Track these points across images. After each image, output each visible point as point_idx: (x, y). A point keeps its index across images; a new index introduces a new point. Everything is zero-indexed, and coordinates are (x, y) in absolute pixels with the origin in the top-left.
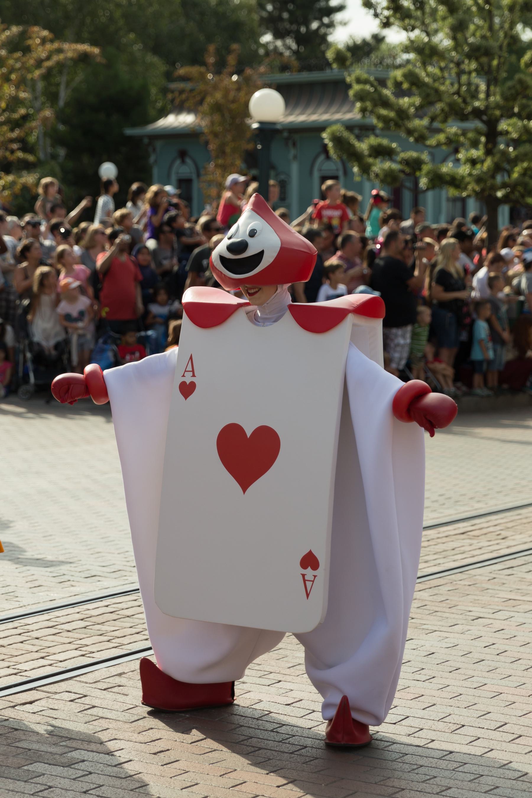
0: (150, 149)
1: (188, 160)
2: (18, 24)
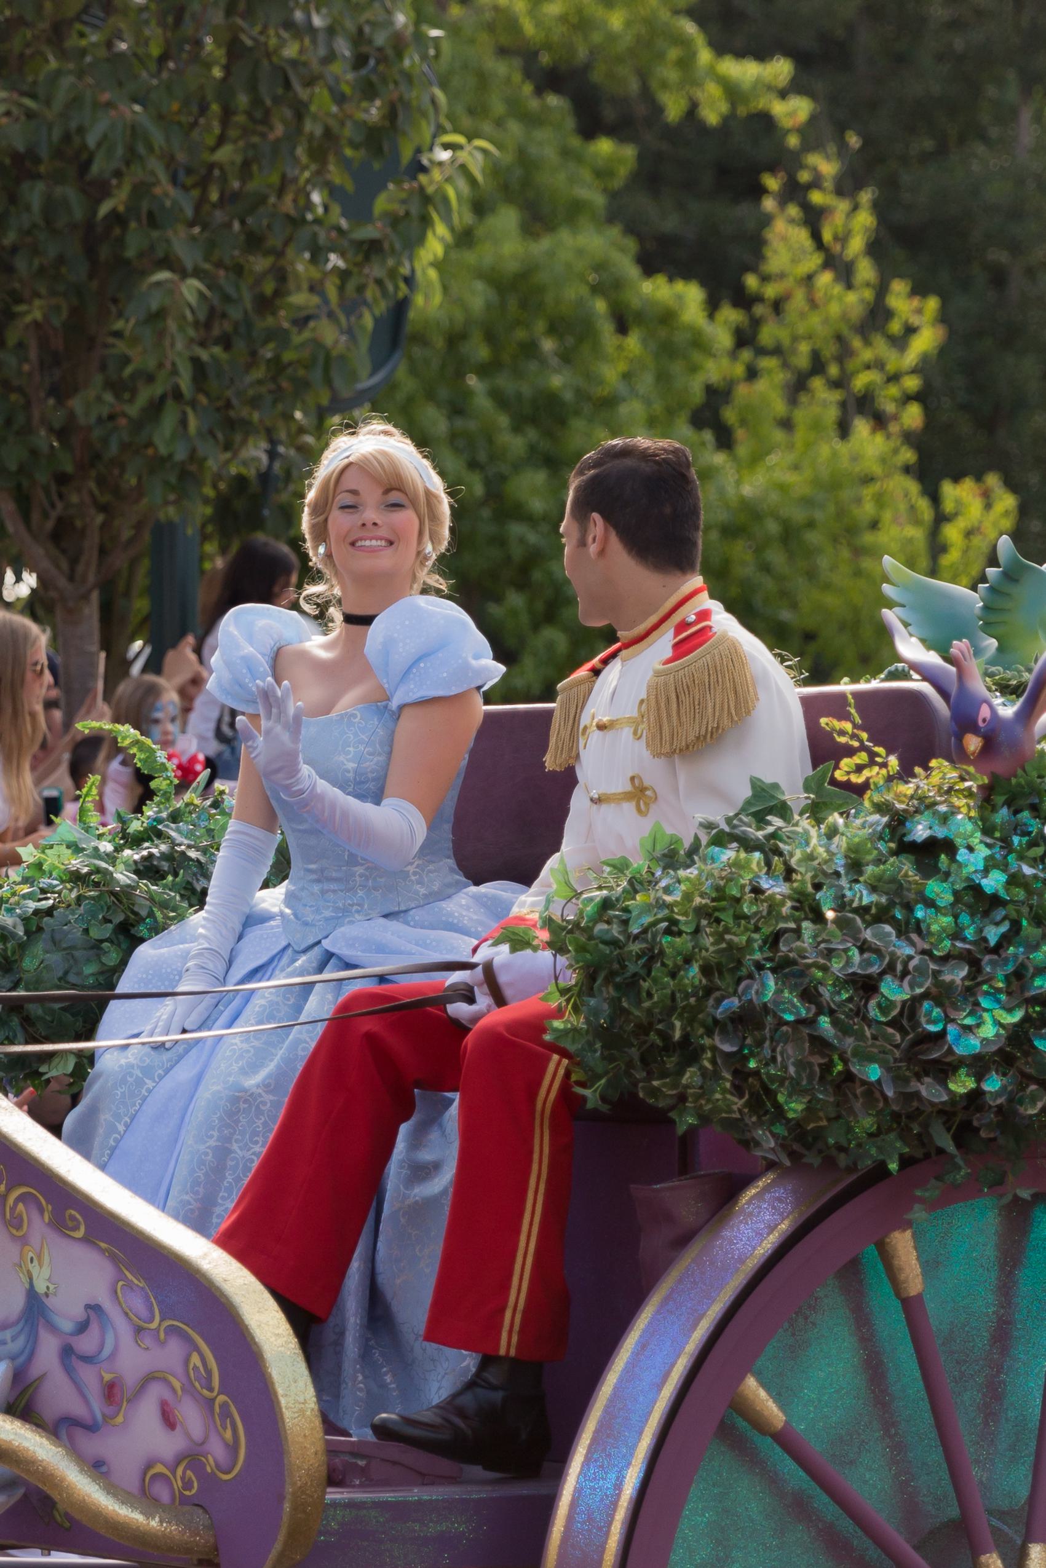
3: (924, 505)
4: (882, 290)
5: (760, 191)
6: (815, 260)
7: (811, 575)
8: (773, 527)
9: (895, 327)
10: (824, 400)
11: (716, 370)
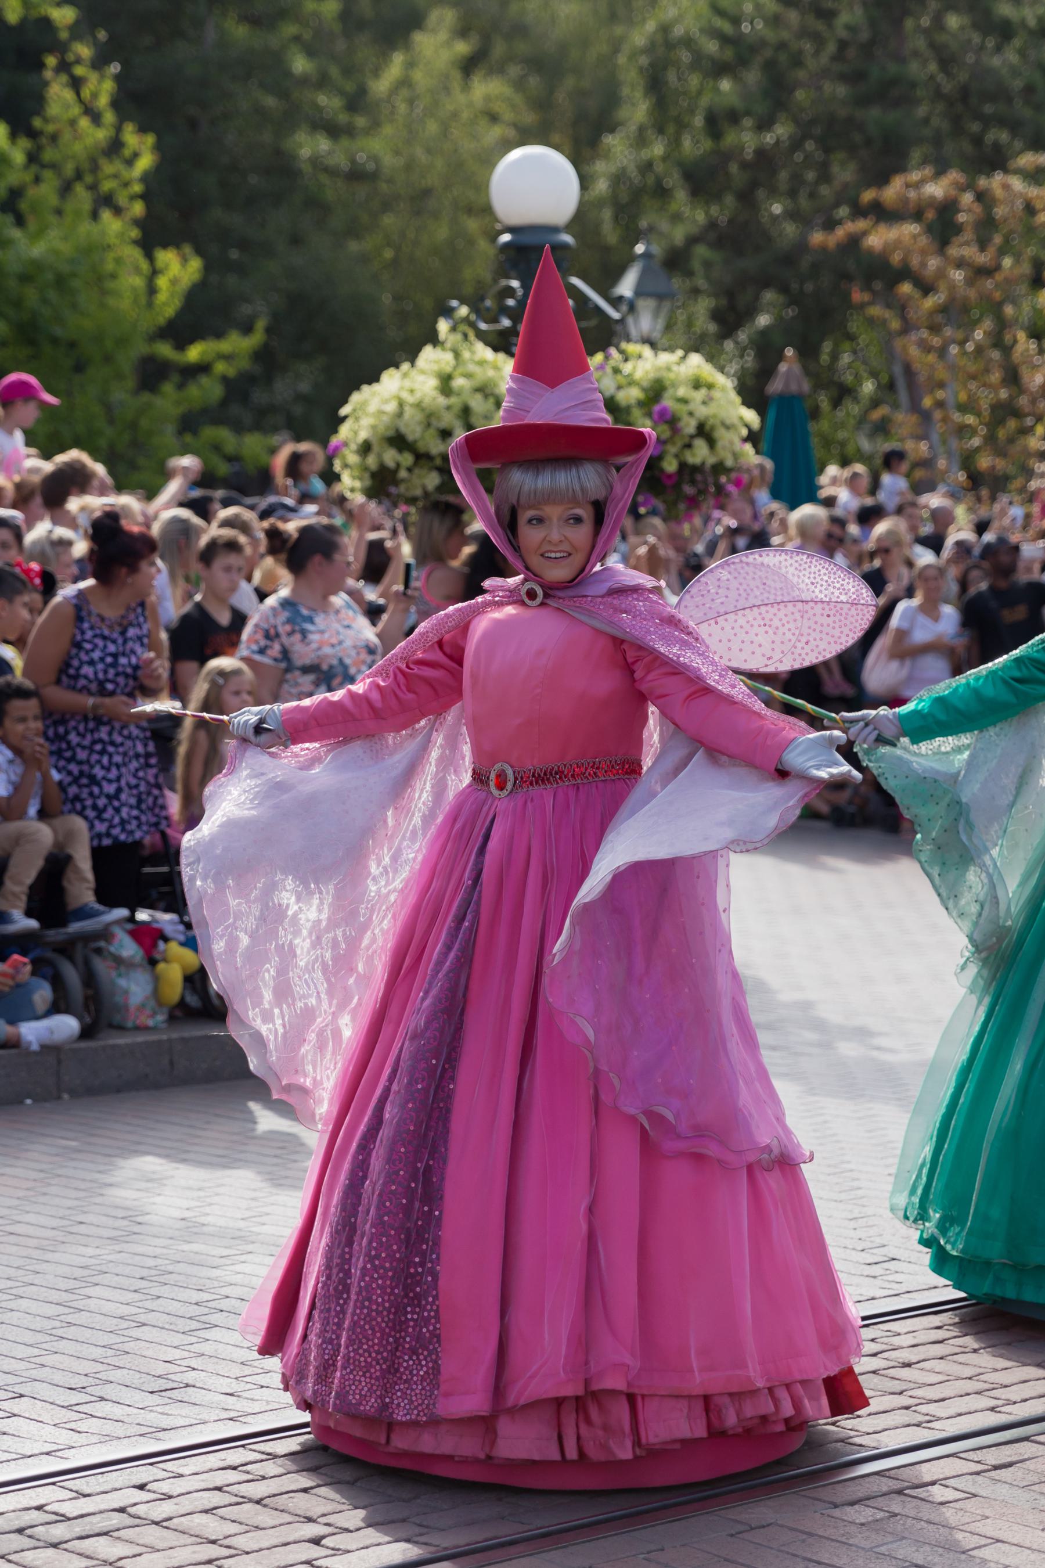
3: (144, 265)
4: (119, 129)
5: (42, 65)
6: (76, 110)
7: (74, 306)
8: (50, 276)
9: (127, 152)
10: (82, 196)
11: (14, 178)
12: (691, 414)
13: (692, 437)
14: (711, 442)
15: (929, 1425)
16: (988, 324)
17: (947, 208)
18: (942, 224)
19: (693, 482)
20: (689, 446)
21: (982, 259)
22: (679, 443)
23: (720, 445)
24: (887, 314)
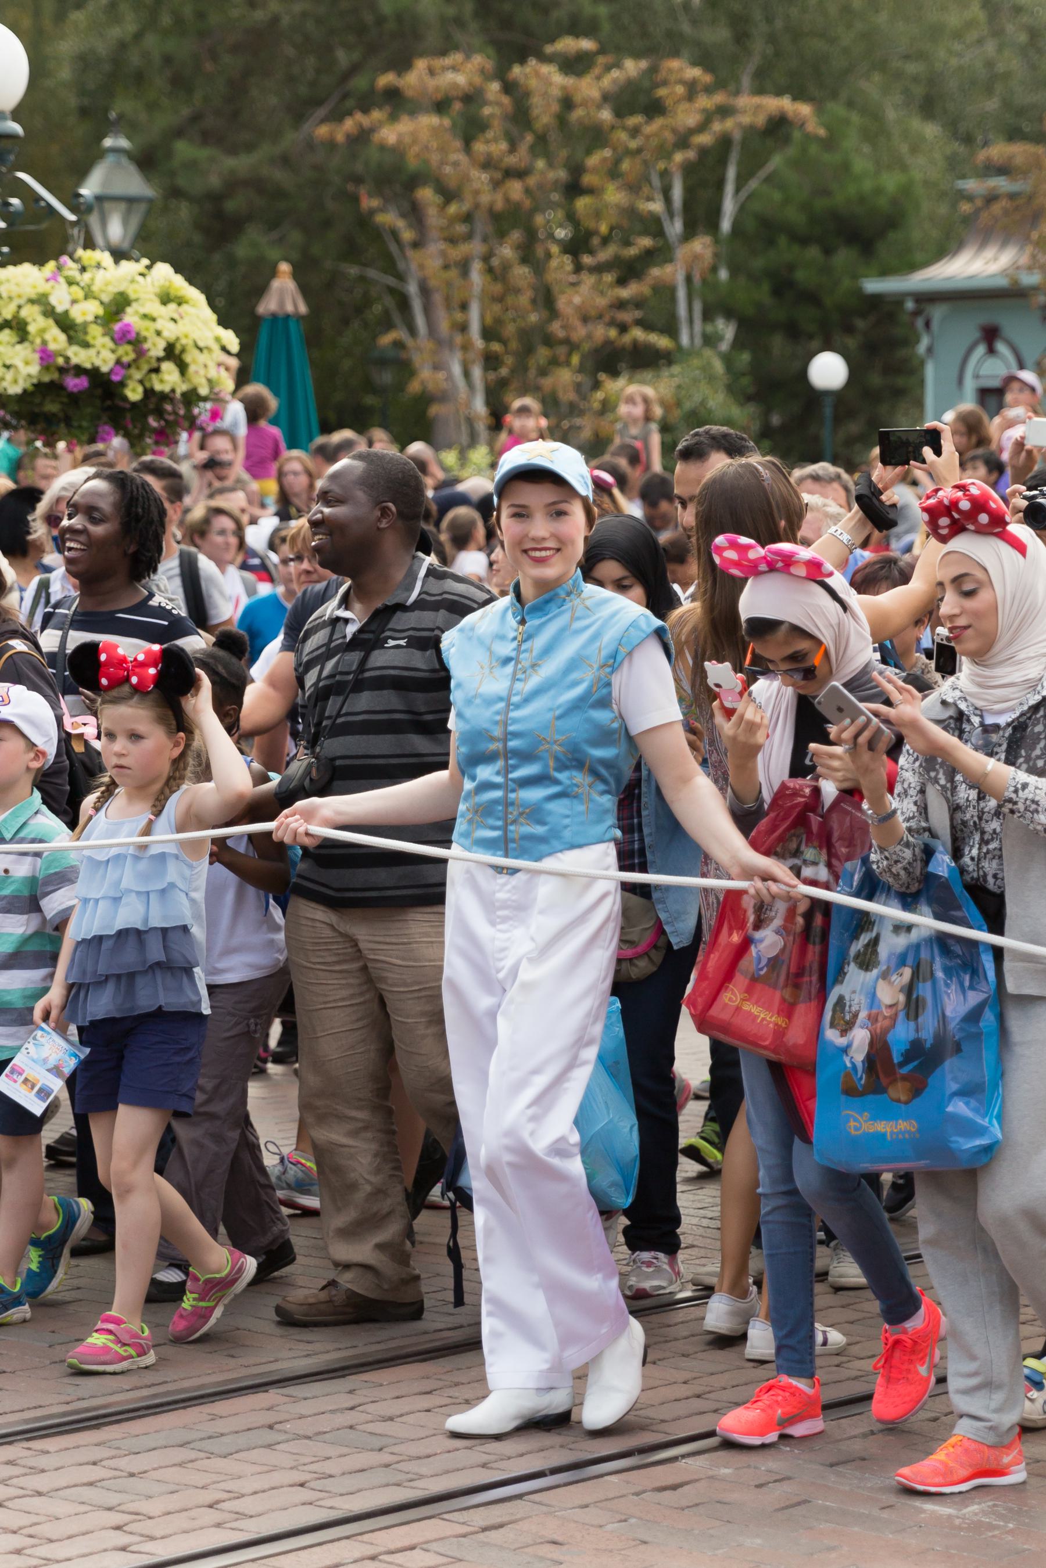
0: (920, 323)
1: (1001, 347)
2: (637, 55)
12: (159, 333)
13: (159, 360)
14: (183, 367)
15: (411, 1484)
16: (516, 235)
17: (472, 98)
18: (467, 118)
19: (159, 413)
20: (157, 370)
21: (512, 160)
22: (145, 368)
23: (192, 369)
24: (401, 224)
